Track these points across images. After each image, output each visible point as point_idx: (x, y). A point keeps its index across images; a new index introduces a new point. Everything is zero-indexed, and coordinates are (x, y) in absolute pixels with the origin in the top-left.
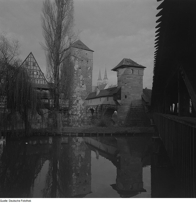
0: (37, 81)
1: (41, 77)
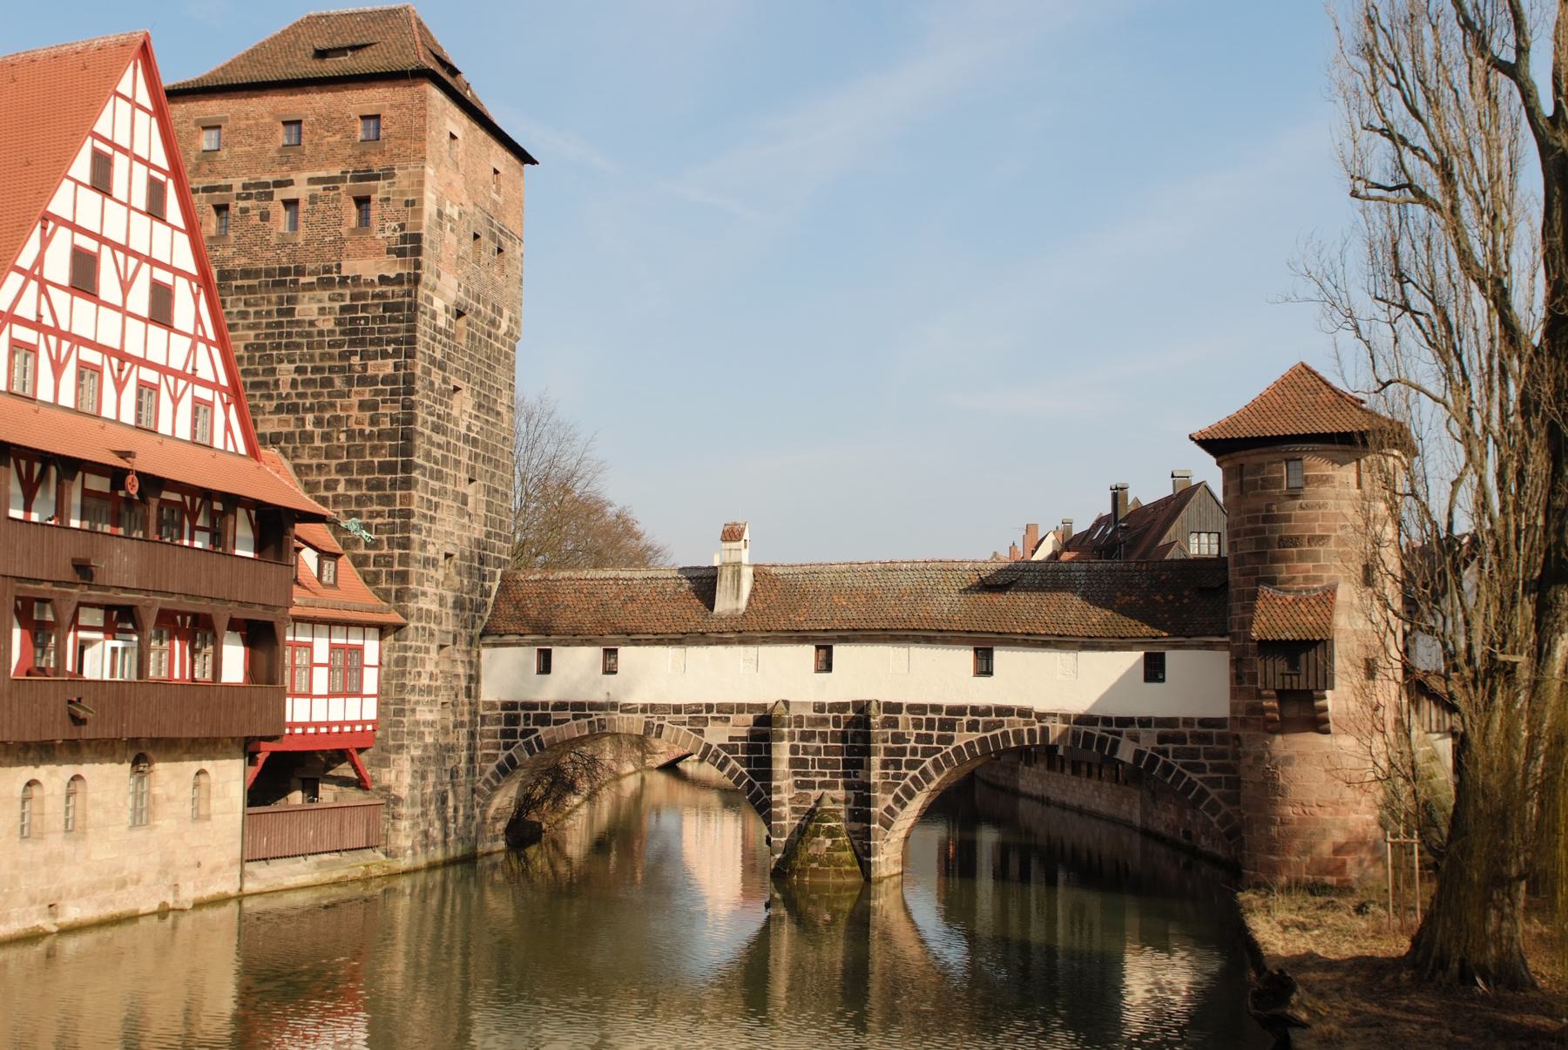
0: (175, 400)
1: (205, 372)
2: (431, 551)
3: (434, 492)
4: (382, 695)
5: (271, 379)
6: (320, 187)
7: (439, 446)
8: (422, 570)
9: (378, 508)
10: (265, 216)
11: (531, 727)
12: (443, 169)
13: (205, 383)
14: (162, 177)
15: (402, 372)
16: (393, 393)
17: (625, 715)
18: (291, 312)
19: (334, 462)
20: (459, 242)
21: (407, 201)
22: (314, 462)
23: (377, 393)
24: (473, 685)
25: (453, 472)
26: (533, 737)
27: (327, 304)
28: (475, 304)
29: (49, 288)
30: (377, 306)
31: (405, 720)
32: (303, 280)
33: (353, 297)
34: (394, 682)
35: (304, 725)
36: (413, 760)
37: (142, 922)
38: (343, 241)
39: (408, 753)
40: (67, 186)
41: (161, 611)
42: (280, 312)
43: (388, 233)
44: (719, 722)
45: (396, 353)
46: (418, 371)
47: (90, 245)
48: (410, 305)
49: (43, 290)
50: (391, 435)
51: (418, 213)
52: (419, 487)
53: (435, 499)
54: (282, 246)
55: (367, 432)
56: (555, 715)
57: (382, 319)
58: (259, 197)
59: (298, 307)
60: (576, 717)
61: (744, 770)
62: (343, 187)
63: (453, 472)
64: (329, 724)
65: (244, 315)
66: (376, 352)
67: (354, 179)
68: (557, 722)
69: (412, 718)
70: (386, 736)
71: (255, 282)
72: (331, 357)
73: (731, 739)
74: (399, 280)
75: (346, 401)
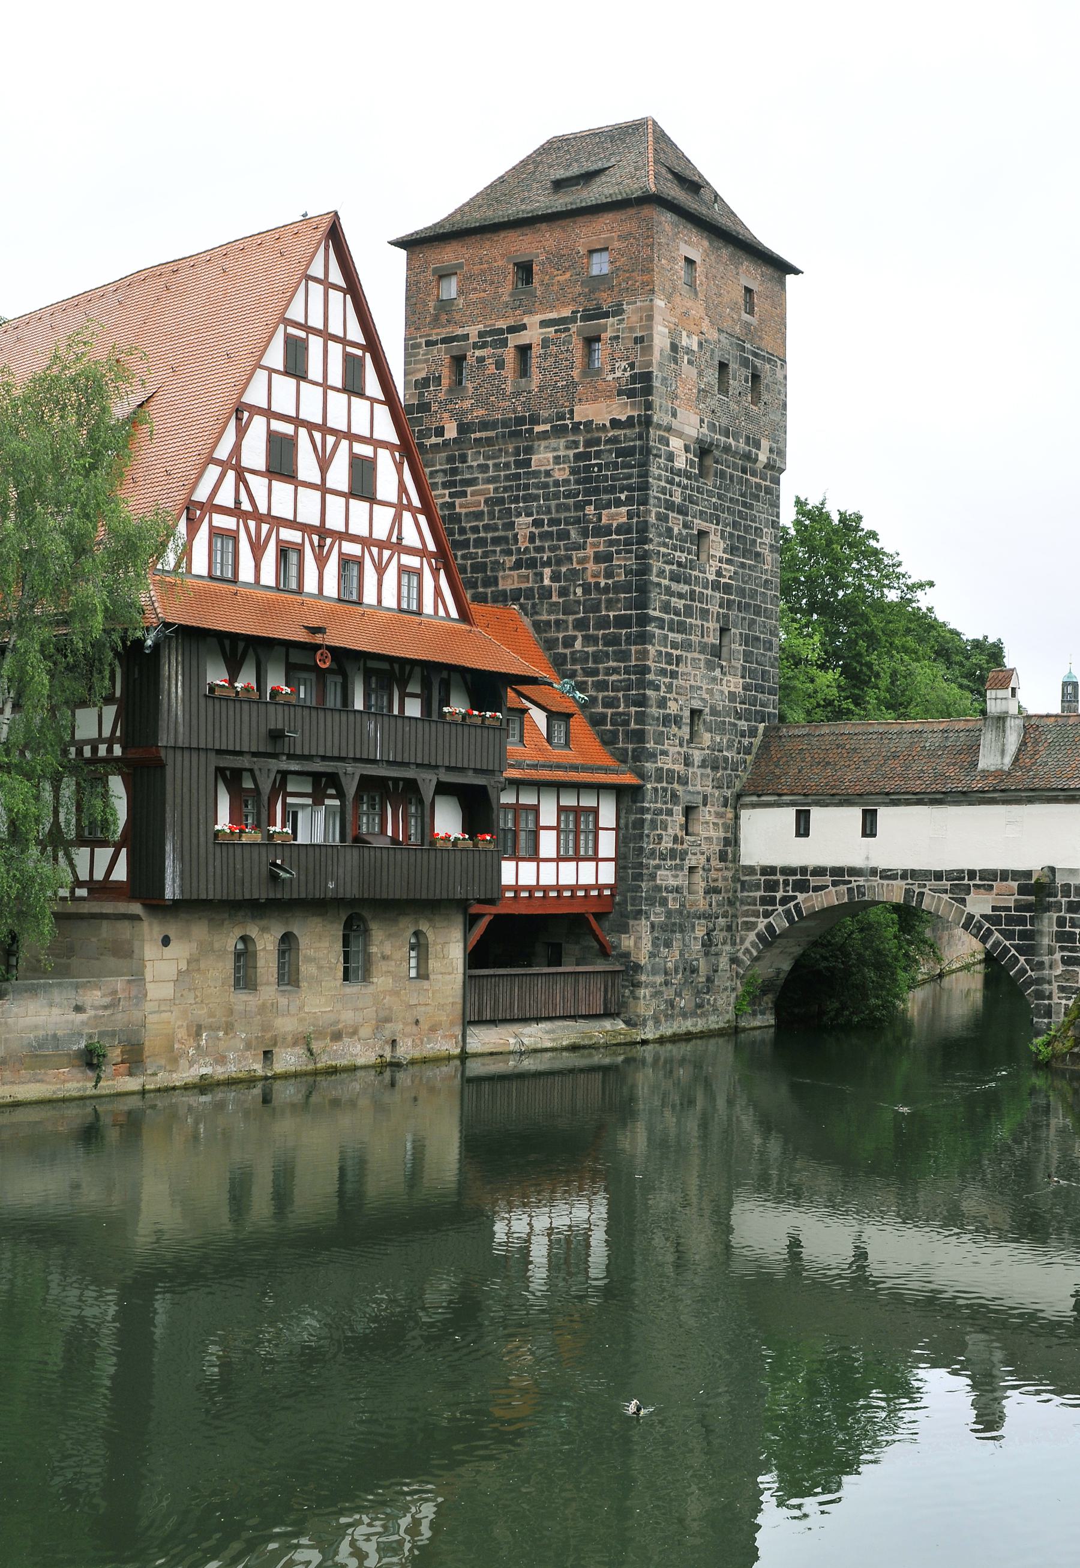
0: (381, 570)
1: (411, 538)
2: (673, 708)
3: (674, 645)
4: (620, 860)
5: (510, 534)
6: (552, 329)
7: (681, 596)
8: (661, 728)
9: (615, 664)
10: (500, 365)
11: (791, 893)
12: (677, 299)
13: (411, 551)
14: (359, 352)
15: (635, 520)
16: (627, 543)
17: (885, 882)
18: (527, 463)
19: (571, 618)
20: (700, 374)
21: (636, 338)
22: (553, 617)
23: (611, 543)
24: (730, 850)
25: (699, 622)
26: (792, 904)
27: (561, 453)
28: (723, 439)
29: (248, 476)
30: (610, 451)
31: (643, 885)
32: (538, 429)
33: (588, 443)
34: (632, 845)
35: (530, 889)
36: (653, 926)
37: (360, 1074)
38: (574, 384)
39: (647, 918)
40: (261, 376)
41: (362, 776)
42: (519, 464)
43: (618, 374)
44: (982, 891)
45: (629, 501)
46: (652, 519)
47: (287, 429)
48: (641, 447)
49: (240, 478)
50: (626, 588)
51: (648, 350)
52: (656, 641)
53: (675, 652)
54: (517, 394)
55: (602, 585)
56: (814, 881)
57: (616, 466)
58: (495, 344)
59: (534, 457)
60: (835, 884)
61: (1007, 943)
62: (573, 328)
63: (699, 622)
64: (559, 888)
65: (484, 468)
66: (610, 500)
67: (585, 318)
68: (817, 889)
69: (651, 883)
70: (625, 901)
71: (491, 434)
72: (567, 508)
73: (994, 908)
74: (630, 422)
75: (581, 554)
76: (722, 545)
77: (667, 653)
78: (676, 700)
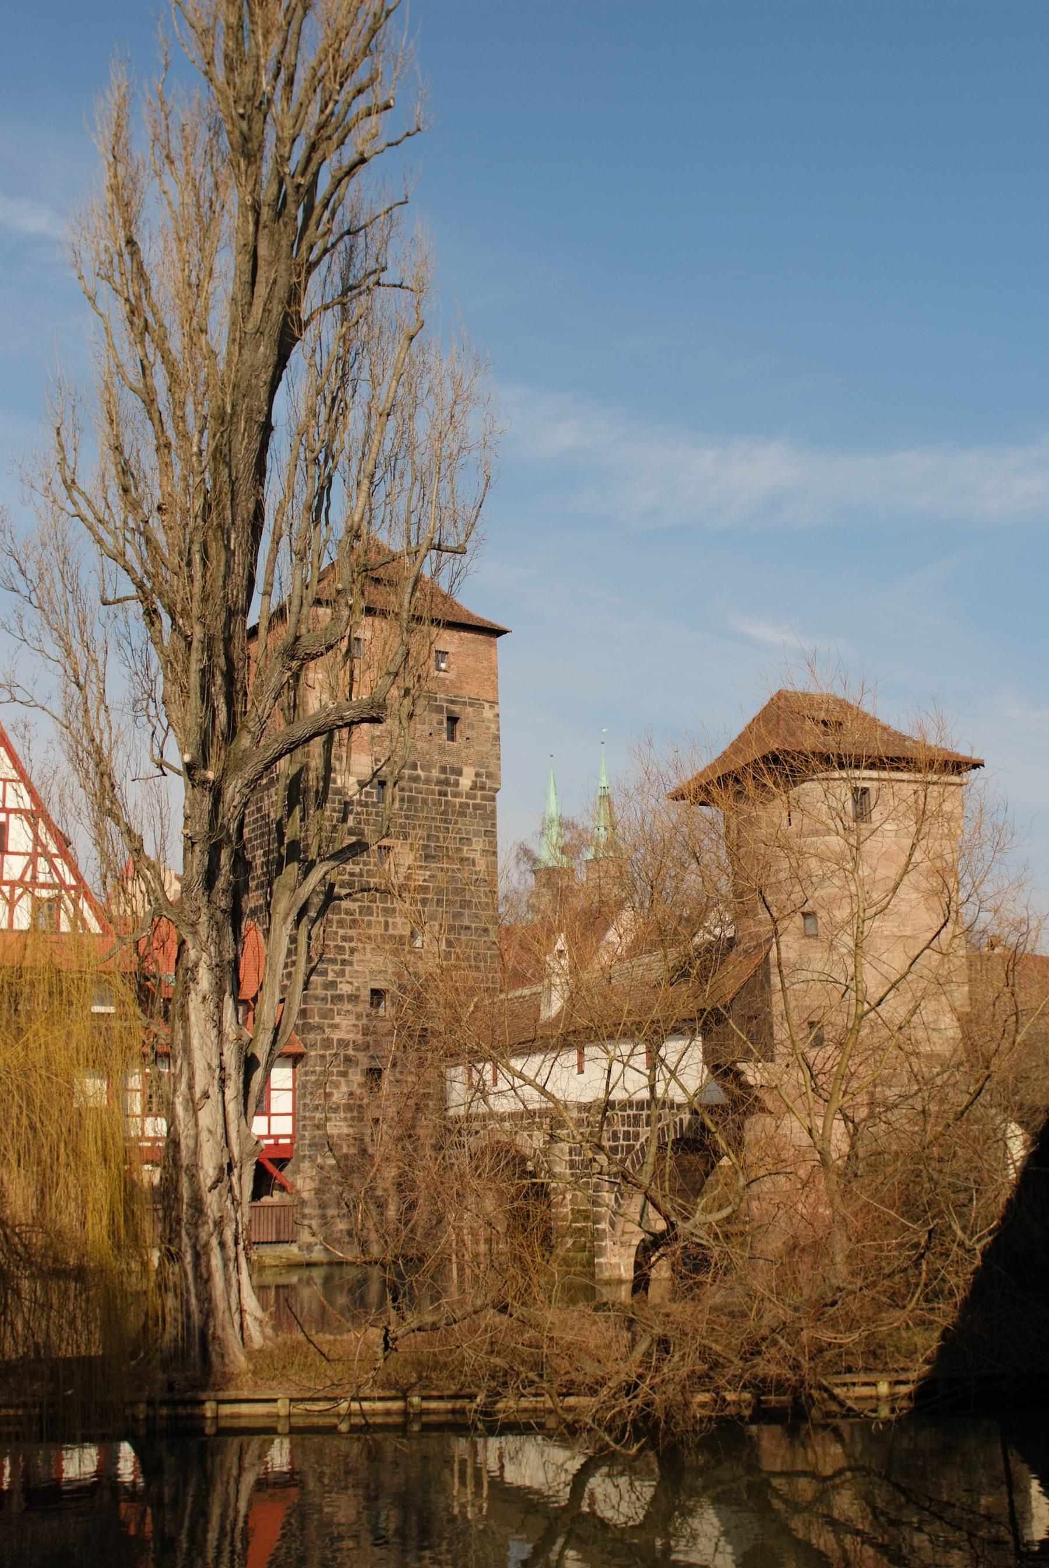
2: (345, 989)
3: (344, 939)
76: (412, 857)
77: (336, 946)
78: (351, 983)
